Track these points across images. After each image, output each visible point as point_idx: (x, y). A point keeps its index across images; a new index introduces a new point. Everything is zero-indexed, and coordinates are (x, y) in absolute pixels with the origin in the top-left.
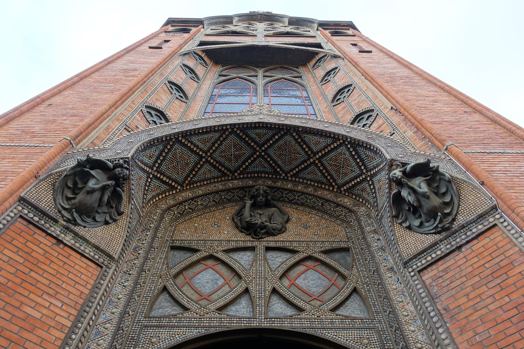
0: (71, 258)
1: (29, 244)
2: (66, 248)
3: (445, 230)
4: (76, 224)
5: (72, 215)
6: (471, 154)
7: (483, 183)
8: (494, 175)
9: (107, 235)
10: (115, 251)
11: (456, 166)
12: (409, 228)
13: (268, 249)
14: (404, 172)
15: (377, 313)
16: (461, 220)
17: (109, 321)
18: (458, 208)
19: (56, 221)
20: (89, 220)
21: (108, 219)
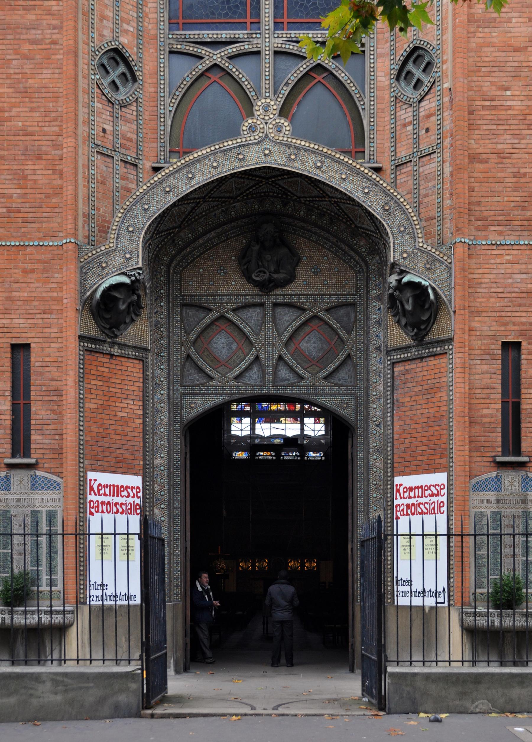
0: (124, 363)
1: (99, 368)
2: (117, 358)
3: (420, 339)
4: (116, 336)
5: (113, 332)
6: (479, 247)
7: (455, 312)
8: (479, 290)
9: (138, 332)
10: (147, 341)
11: (451, 276)
12: (398, 322)
13: (276, 305)
14: (399, 281)
15: (361, 380)
16: (428, 338)
17: (161, 402)
18: (432, 325)
19: (105, 341)
20: (122, 326)
21: (133, 316)
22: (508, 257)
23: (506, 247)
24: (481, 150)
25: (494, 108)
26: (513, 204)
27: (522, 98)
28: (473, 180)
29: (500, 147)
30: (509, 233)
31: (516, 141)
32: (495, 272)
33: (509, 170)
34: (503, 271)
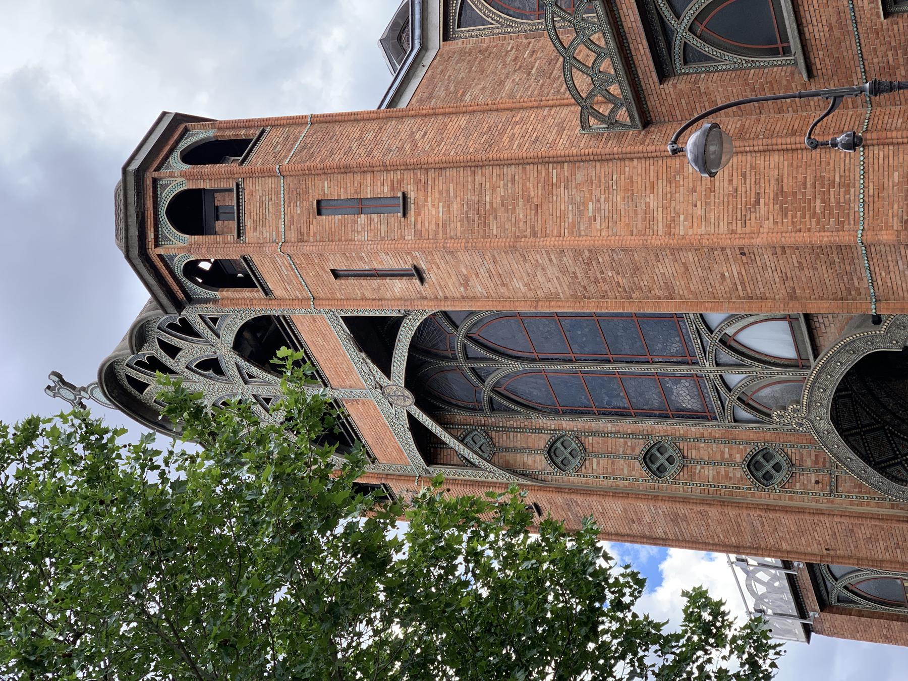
22: (883, 274)
23: (874, 276)
24: (783, 291)
25: (743, 283)
26: (830, 271)
27: (728, 265)
28: (812, 297)
29: (777, 279)
30: (858, 273)
31: (769, 269)
32: (899, 283)
33: (798, 273)
34: (898, 278)
